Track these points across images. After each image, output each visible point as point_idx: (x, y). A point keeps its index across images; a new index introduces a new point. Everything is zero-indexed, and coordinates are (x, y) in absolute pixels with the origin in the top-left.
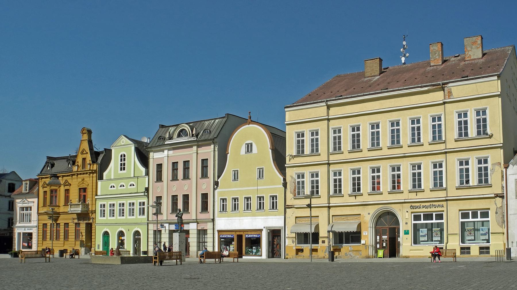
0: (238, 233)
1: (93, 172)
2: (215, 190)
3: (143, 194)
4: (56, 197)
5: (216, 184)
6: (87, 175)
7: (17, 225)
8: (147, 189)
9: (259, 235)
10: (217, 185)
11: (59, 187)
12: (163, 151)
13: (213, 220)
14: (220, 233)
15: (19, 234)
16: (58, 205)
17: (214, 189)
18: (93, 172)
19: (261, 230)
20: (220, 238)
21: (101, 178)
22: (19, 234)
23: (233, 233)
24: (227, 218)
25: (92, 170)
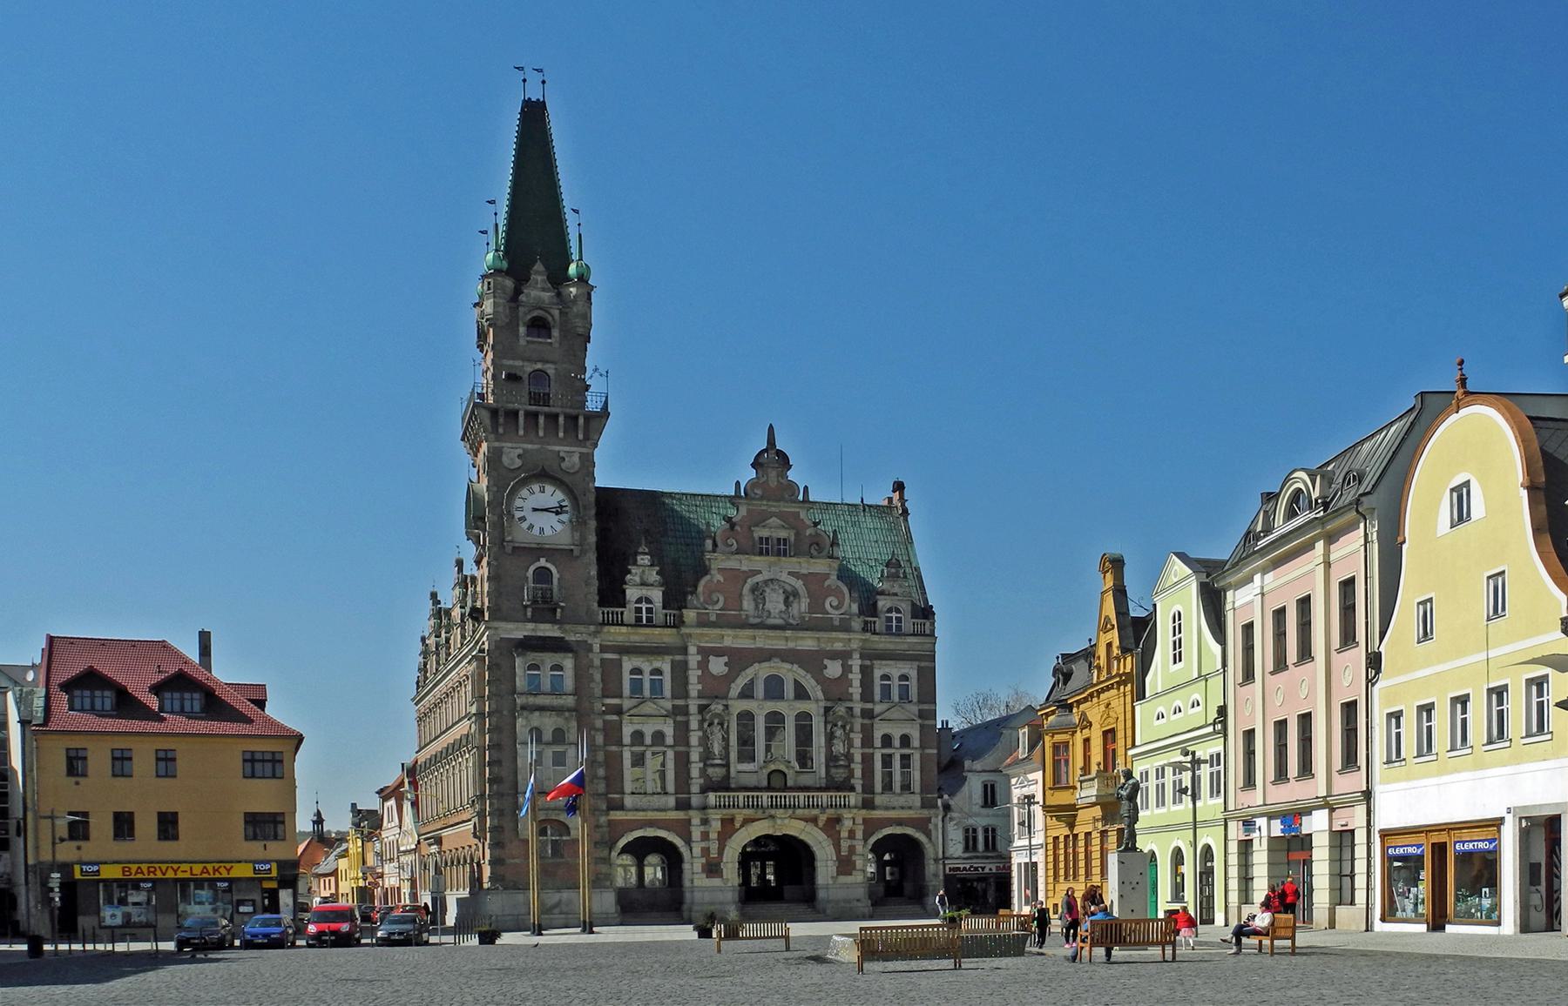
0: (1437, 838)
1: (1125, 679)
2: (1373, 685)
3: (1210, 729)
4: (1067, 761)
5: (1374, 661)
6: (1114, 692)
7: (1015, 845)
8: (1222, 711)
9: (1494, 840)
10: (1378, 671)
11: (1073, 735)
12: (1250, 580)
13: (1368, 795)
14: (1391, 841)
15: (1019, 865)
16: (1071, 784)
17: (1370, 682)
18: (1125, 679)
19: (1498, 823)
20: (1388, 859)
21: (1140, 694)
22: (1019, 865)
23: (1421, 839)
24: (1403, 785)
25: (1121, 676)
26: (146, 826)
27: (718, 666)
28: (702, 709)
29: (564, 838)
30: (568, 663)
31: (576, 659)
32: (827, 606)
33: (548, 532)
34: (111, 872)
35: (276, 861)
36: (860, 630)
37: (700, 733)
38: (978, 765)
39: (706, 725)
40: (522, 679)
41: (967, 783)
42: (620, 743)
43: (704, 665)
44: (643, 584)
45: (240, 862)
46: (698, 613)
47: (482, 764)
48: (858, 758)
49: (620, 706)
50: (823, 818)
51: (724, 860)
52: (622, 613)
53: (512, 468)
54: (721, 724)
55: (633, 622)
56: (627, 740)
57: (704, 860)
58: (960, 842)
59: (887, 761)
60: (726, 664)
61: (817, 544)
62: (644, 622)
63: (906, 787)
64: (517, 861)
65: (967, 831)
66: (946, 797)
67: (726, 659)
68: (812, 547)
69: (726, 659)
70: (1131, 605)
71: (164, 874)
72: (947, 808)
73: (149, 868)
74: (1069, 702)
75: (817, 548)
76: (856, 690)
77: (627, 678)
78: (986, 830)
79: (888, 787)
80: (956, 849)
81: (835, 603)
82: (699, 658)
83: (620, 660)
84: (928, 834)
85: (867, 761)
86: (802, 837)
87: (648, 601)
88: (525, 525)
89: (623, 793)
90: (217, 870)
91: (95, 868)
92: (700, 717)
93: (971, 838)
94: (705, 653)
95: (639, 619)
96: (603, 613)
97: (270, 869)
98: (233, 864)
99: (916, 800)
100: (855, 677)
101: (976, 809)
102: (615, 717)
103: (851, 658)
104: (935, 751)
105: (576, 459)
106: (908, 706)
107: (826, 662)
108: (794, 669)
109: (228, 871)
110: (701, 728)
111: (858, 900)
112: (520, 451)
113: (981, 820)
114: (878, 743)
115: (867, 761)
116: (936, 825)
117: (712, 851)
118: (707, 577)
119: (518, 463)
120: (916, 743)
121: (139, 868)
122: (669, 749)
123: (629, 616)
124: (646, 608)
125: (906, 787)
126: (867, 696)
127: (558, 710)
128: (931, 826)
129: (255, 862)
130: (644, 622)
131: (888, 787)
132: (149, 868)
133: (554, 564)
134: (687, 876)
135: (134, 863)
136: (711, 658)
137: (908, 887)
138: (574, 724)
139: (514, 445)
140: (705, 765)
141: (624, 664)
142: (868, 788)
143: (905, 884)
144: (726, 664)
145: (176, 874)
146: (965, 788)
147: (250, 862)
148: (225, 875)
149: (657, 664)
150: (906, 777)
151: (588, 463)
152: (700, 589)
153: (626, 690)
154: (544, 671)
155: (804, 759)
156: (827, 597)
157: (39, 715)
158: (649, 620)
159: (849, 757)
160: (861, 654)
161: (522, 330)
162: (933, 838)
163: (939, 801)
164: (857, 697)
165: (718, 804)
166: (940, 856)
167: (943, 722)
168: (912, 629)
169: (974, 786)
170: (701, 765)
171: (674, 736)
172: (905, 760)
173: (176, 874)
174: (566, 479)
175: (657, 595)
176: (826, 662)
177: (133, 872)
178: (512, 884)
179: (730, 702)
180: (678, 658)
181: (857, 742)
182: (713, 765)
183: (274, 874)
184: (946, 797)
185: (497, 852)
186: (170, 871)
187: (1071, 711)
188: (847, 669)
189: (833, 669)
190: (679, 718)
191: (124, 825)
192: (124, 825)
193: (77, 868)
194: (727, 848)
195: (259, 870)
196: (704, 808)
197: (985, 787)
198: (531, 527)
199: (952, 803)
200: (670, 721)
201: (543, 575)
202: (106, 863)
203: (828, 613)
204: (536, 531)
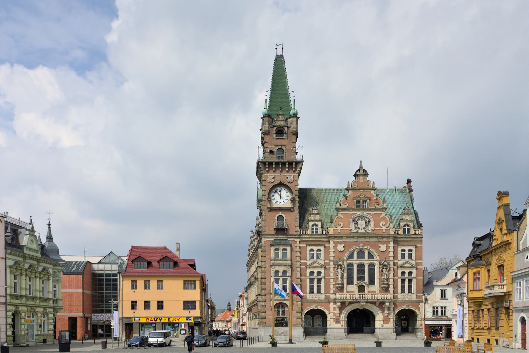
26: (154, 305)
27: (340, 248)
28: (335, 264)
30: (288, 248)
31: (291, 246)
32: (381, 225)
33: (282, 203)
34: (143, 320)
35: (193, 317)
36: (394, 234)
38: (439, 284)
41: (434, 290)
42: (305, 275)
43: (335, 247)
44: (315, 220)
45: (182, 317)
46: (333, 229)
48: (392, 281)
49: (306, 262)
50: (378, 304)
52: (307, 230)
53: (271, 182)
55: (311, 233)
56: (308, 275)
58: (431, 312)
59: (403, 281)
60: (343, 247)
61: (378, 203)
62: (315, 233)
63: (410, 290)
64: (270, 317)
65: (434, 307)
66: (426, 295)
68: (376, 204)
69: (343, 245)
70: (512, 212)
71: (156, 321)
72: (426, 300)
73: (147, 319)
74: (480, 255)
75: (377, 204)
76: (391, 254)
77: (308, 252)
78: (442, 308)
79: (403, 290)
80: (429, 315)
81: (384, 224)
82: (334, 245)
84: (419, 309)
85: (395, 281)
86: (370, 310)
87: (316, 225)
88: (275, 201)
90: (175, 320)
91: (139, 319)
93: (435, 311)
94: (336, 243)
95: (313, 232)
96: (301, 230)
97: (191, 319)
98: (180, 318)
99: (414, 298)
100: (391, 249)
101: (438, 300)
103: (390, 243)
104: (422, 278)
105: (292, 178)
106: (412, 262)
107: (380, 245)
108: (368, 248)
109: (178, 320)
111: (391, 333)
112: (274, 177)
113: (440, 303)
114: (399, 275)
115: (395, 281)
116: (422, 306)
118: (338, 216)
119: (273, 180)
120: (414, 275)
121: (151, 319)
123: (310, 232)
124: (316, 228)
125: (410, 290)
126: (395, 257)
127: (285, 265)
128: (420, 306)
129: (186, 317)
130: (315, 233)
131: (403, 290)
132: (147, 319)
133: (284, 214)
134: (328, 323)
135: (150, 317)
136: (338, 245)
137: (410, 329)
139: (271, 175)
142: (395, 292)
143: (409, 328)
145: (178, 321)
146: (434, 292)
147: (185, 317)
148: (177, 321)
150: (410, 288)
151: (296, 181)
152: (334, 221)
153: (308, 258)
154: (280, 251)
155: (372, 281)
156: (380, 222)
157: (124, 270)
158: (317, 232)
159: (388, 280)
160: (393, 242)
161: (275, 135)
162: (420, 310)
163: (423, 297)
164: (392, 258)
166: (423, 317)
167: (425, 267)
168: (413, 233)
169: (437, 292)
172: (410, 281)
173: (178, 321)
174: (289, 185)
175: (319, 224)
176: (380, 245)
177: (150, 320)
181: (392, 275)
183: (192, 321)
184: (426, 295)
186: (158, 319)
187: (481, 259)
188: (388, 247)
189: (383, 248)
191: (147, 304)
192: (147, 304)
193: (133, 319)
195: (187, 320)
197: (442, 291)
198: (277, 202)
199: (428, 297)
200: (324, 269)
201: (280, 218)
202: (142, 317)
203: (382, 228)
204: (278, 203)
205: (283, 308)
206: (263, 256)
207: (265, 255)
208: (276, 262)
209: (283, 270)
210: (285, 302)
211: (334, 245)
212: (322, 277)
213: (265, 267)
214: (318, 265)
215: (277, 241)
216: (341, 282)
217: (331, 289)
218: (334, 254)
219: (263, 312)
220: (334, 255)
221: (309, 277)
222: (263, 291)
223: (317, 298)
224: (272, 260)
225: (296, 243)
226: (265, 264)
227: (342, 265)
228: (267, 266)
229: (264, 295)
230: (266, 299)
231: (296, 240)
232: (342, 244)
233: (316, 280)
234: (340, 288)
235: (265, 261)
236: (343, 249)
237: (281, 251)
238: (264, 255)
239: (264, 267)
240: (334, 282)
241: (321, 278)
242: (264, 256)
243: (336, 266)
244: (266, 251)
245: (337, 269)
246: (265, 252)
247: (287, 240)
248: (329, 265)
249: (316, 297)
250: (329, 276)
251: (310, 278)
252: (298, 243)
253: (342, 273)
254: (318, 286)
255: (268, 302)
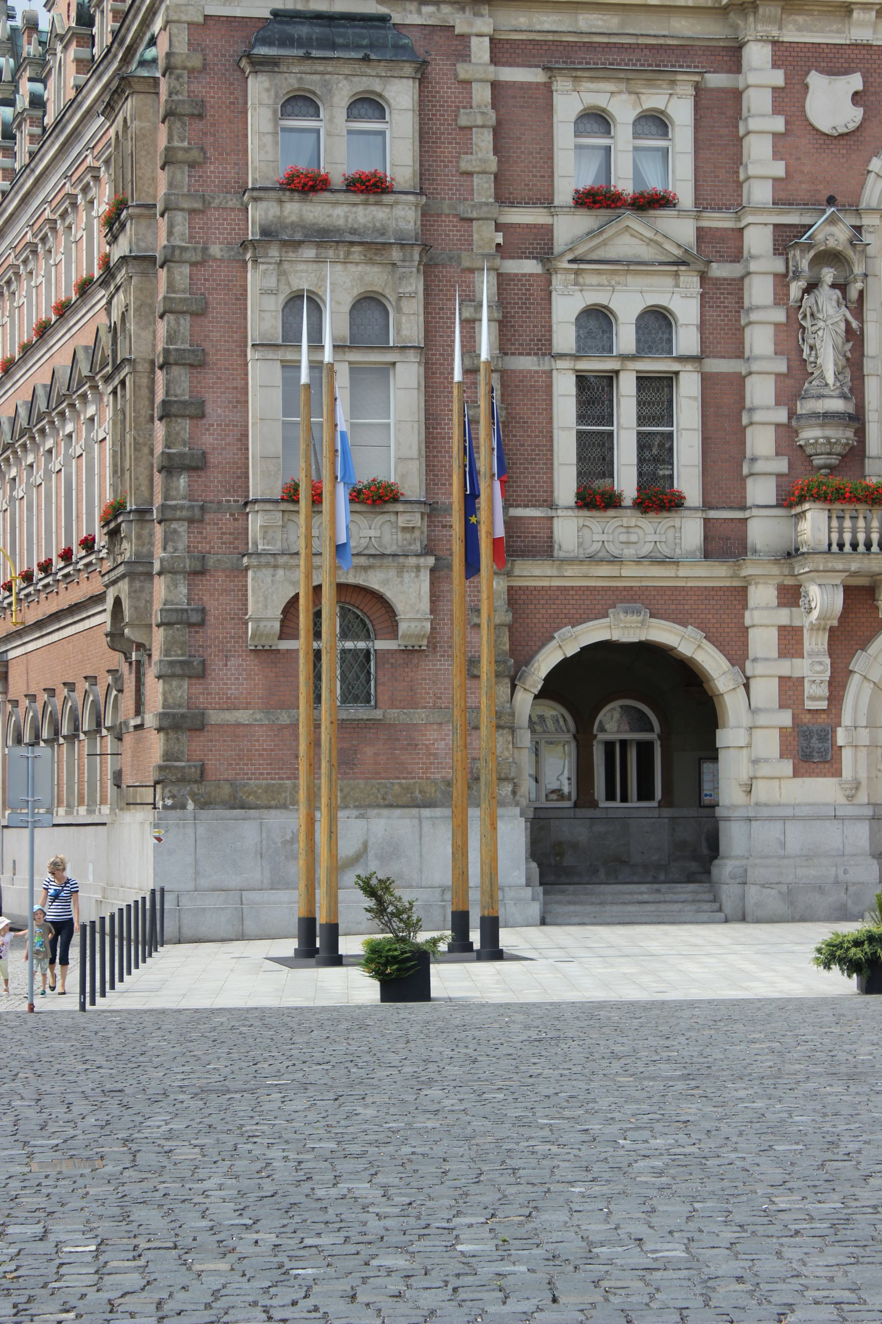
29: (381, 645)
31: (422, 78)
37: (780, 316)
39: (795, 289)
40: (268, 139)
47: (145, 412)
49: (548, 230)
51: (847, 718)
54: (841, 286)
57: (786, 718)
64: (243, 716)
67: (856, 82)
69: (856, 82)
82: (778, 78)
83: (548, 89)
89: (551, 505)
92: (778, 266)
102: (531, 267)
110: (781, 297)
117: (809, 689)
122: (689, 367)
136: (815, 79)
138: (416, 285)
140: (792, 414)
141: (559, 101)
144: (857, 99)
149: (654, 100)
154: (331, 120)
165: (835, 536)
170: (782, 416)
171: (702, 327)
178: (226, 790)
179: (867, 220)
180: (717, 80)
182: (827, 418)
185: (182, 690)
190: (719, 270)
194: (855, 680)
196: (792, 554)
200: (691, 282)
205: (356, 637)
206: (180, 155)
207: (195, 155)
208: (294, 218)
209: (356, 292)
210: (374, 581)
211: (778, 78)
212: (682, 359)
213: (197, 257)
214: (646, 253)
215: (303, 30)
216: (837, 405)
217: (759, 467)
218: (777, 155)
219: (178, 670)
220: (779, 169)
221: (576, 357)
222: (182, 481)
223: (646, 550)
224: (260, 192)
225: (464, 55)
226: (191, 237)
227: (850, 253)
228: (215, 250)
229: (185, 513)
230: (204, 547)
231: (461, 22)
232: (847, 72)
233: (627, 386)
234: (834, 461)
235: (198, 205)
236: (852, 116)
237: (341, 114)
238: (186, 150)
239: (187, 256)
240: (778, 403)
241: (676, 367)
242: (192, 165)
243: (804, 265)
244: (200, 116)
245: (812, 287)
246: (198, 125)
247: (384, 19)
248: (737, 256)
249: (633, 538)
250: (739, 353)
251: (584, 365)
252: (480, 49)
253: (847, 323)
254: (644, 442)
255: (221, 577)
